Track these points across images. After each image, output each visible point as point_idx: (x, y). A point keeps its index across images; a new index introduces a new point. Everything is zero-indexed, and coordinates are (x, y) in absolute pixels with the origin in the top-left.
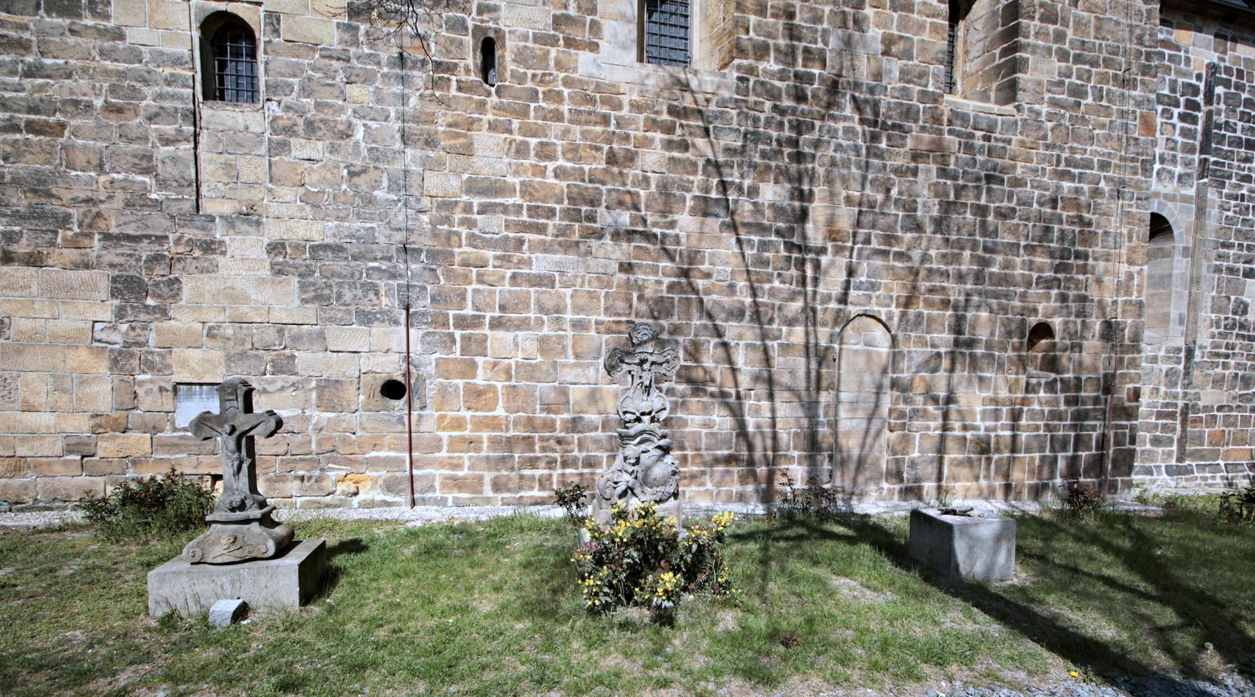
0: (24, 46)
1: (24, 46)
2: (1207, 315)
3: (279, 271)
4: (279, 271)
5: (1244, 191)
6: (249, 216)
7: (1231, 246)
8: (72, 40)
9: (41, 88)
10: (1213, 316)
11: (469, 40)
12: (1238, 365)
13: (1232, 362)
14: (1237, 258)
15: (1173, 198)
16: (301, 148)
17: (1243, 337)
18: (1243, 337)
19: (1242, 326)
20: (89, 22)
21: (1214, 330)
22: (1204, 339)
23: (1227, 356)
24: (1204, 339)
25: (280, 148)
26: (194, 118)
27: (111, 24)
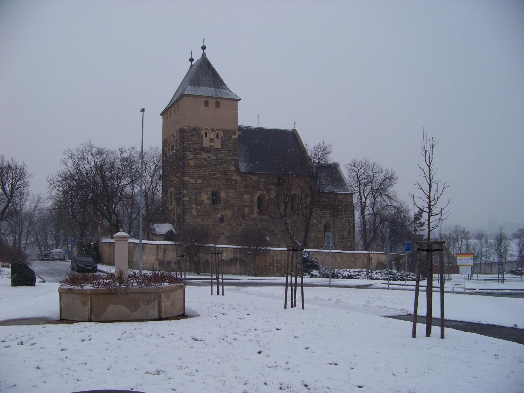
2: (337, 237)
3: (226, 239)
4: (226, 239)
5: (342, 218)
6: (223, 234)
7: (341, 226)
10: (338, 237)
11: (242, 215)
12: (344, 244)
13: (342, 244)
14: (342, 228)
15: (329, 220)
16: (228, 227)
17: (344, 240)
18: (344, 240)
19: (344, 238)
21: (339, 239)
22: (337, 240)
23: (341, 243)
24: (337, 240)
25: (225, 227)
26: (219, 225)
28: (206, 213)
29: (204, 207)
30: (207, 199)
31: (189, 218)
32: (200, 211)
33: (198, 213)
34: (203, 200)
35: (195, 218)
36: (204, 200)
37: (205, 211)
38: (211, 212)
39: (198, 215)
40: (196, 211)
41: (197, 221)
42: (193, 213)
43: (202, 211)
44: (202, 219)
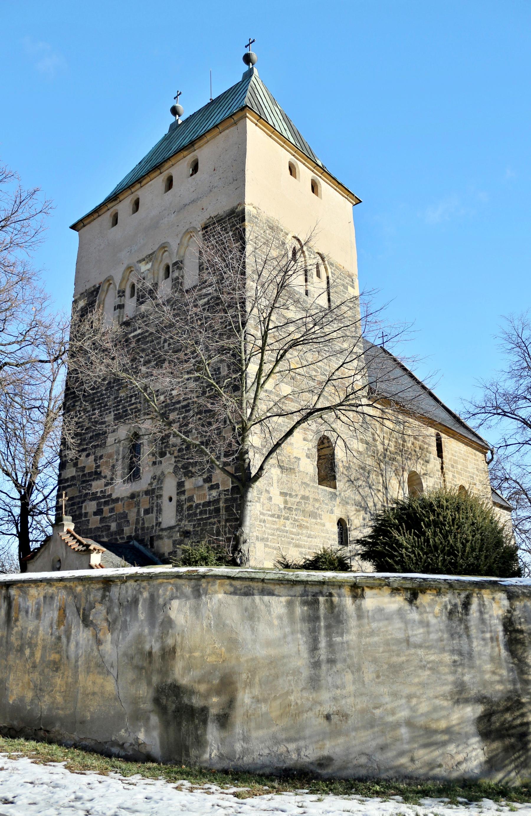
0: (307, 528)
1: (307, 528)
8: (316, 526)
9: (311, 542)
20: (319, 521)
27: (323, 521)
28: (305, 503)
29: (300, 482)
30: (308, 457)
31: (262, 514)
32: (291, 495)
33: (286, 502)
34: (295, 457)
35: (279, 517)
36: (298, 456)
37: (304, 497)
38: (317, 505)
39: (285, 507)
40: (283, 494)
41: (283, 531)
42: (274, 501)
43: (297, 495)
44: (297, 523)
